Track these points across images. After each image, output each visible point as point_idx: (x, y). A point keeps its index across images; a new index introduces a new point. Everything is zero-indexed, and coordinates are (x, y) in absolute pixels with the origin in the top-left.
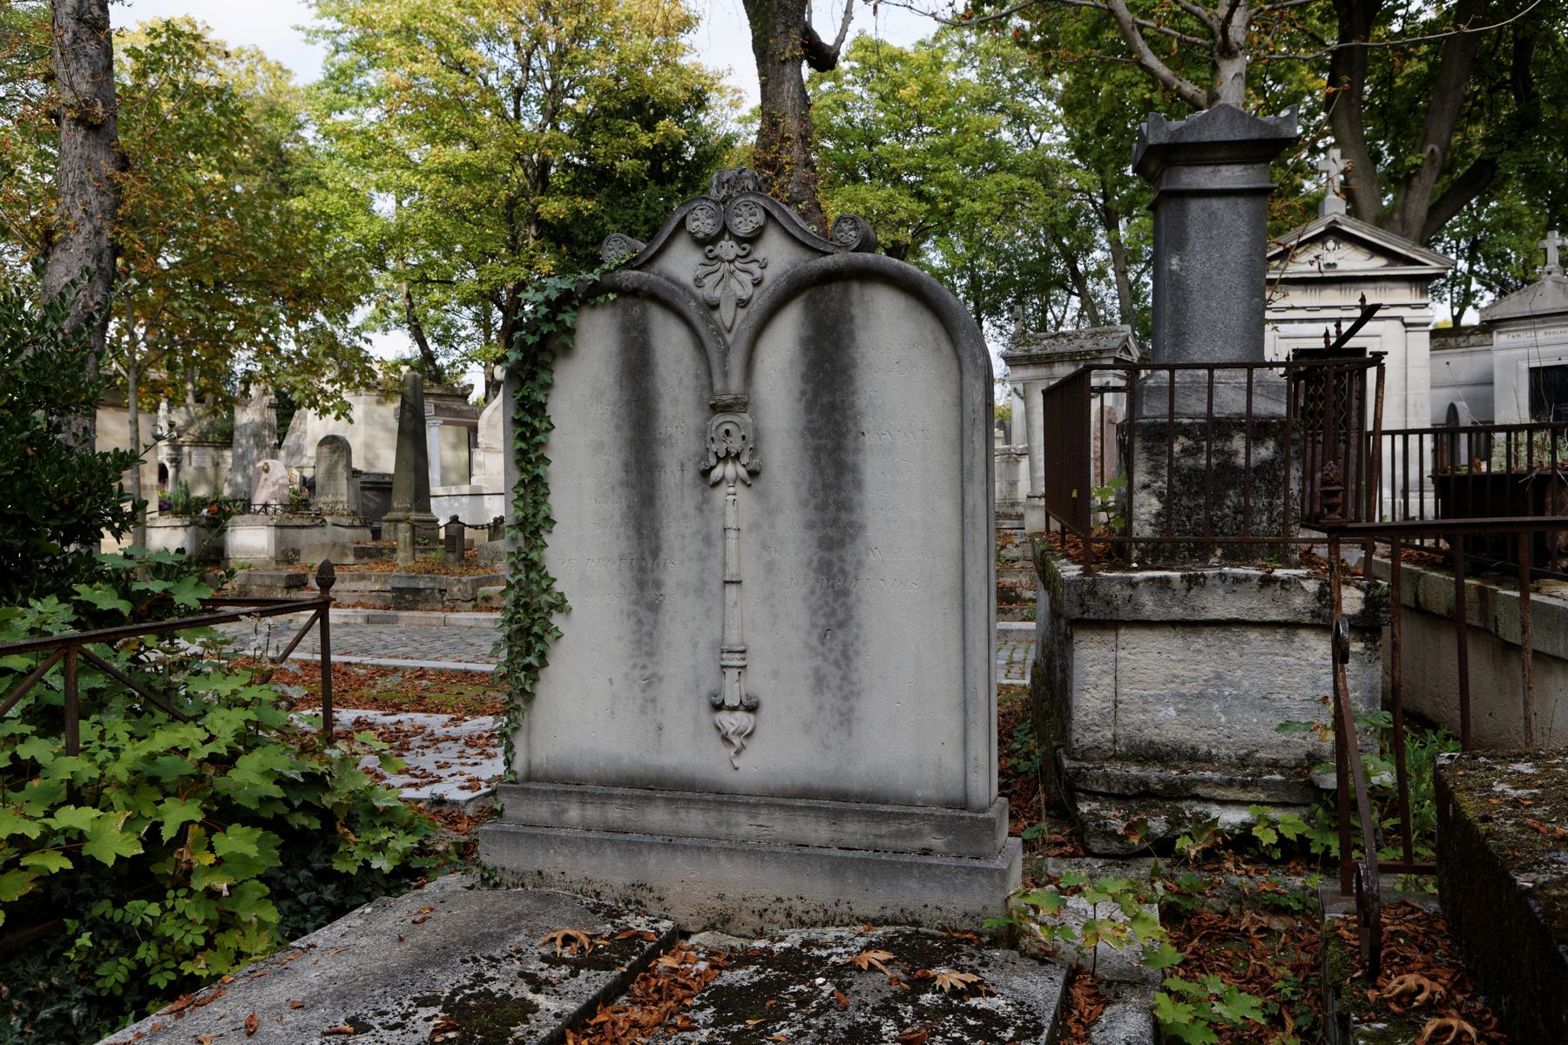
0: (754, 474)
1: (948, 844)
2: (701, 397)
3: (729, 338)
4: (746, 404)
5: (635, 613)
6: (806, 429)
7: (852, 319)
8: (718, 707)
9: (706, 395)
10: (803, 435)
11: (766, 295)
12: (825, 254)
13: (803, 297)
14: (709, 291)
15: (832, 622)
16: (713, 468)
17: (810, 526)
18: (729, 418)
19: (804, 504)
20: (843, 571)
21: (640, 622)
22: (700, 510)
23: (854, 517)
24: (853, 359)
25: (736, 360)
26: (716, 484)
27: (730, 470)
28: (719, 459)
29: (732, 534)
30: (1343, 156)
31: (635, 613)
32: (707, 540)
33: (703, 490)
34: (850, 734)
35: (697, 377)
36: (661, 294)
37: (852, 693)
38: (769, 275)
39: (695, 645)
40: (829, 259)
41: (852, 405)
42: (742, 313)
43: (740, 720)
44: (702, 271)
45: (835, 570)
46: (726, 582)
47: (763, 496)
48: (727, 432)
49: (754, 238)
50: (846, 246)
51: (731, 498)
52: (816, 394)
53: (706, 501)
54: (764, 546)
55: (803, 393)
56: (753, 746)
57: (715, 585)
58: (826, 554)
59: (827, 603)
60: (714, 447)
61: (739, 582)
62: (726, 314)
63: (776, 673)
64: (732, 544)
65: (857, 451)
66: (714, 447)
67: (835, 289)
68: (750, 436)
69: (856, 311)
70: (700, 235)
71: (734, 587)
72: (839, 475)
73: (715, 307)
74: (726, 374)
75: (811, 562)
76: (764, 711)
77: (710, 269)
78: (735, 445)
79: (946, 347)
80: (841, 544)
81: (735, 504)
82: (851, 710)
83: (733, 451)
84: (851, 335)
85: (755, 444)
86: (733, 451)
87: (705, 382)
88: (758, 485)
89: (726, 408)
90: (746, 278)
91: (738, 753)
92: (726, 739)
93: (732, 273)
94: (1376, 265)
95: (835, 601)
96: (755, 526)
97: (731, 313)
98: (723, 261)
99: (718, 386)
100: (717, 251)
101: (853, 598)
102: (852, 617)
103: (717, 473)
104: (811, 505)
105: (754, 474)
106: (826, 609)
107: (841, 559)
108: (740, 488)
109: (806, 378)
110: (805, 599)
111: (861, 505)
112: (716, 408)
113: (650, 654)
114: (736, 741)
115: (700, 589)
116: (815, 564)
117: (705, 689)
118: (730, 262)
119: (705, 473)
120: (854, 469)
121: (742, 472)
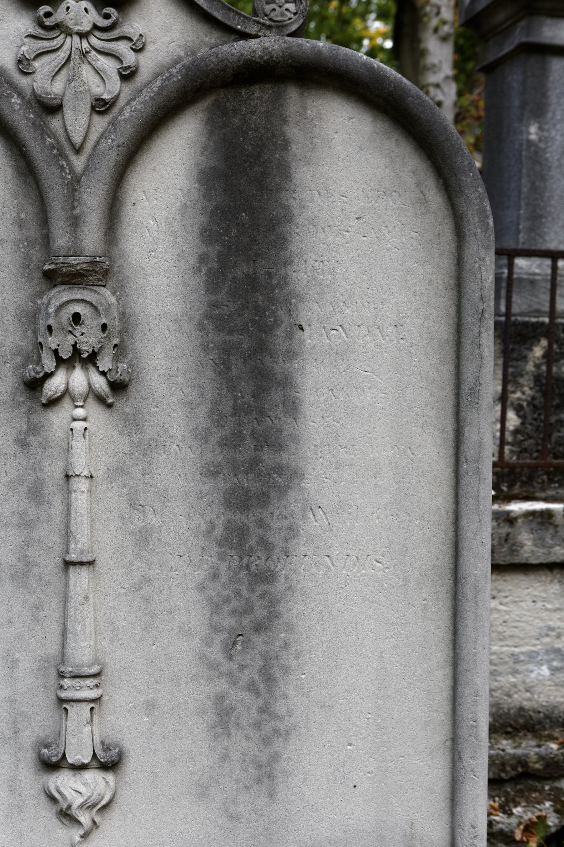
0: (118, 387)
2: (27, 258)
3: (78, 163)
4: (106, 273)
6: (206, 316)
7: (286, 144)
8: (50, 766)
9: (36, 254)
10: (201, 327)
11: (147, 95)
12: (246, 36)
13: (207, 103)
14: (45, 80)
15: (246, 622)
16: (49, 376)
18: (78, 294)
19: (203, 436)
20: (265, 543)
22: (23, 443)
23: (285, 458)
24: (287, 209)
25: (93, 200)
26: (53, 402)
27: (78, 379)
28: (60, 361)
29: (82, 485)
32: (36, 494)
33: (29, 412)
34: (272, 795)
35: (20, 223)
37: (276, 732)
38: (148, 63)
39: (13, 665)
40: (253, 43)
41: (284, 282)
42: (100, 123)
43: (95, 783)
44: (29, 48)
45: (253, 541)
46: (68, 564)
47: (133, 423)
48: (76, 318)
50: (278, 27)
51: (79, 425)
52: (224, 263)
53: (34, 429)
54: (134, 504)
55: (203, 259)
56: (111, 824)
57: (50, 567)
58: (238, 517)
59: (237, 593)
60: (52, 342)
61: (91, 563)
62: (76, 121)
63: (151, 706)
64: (81, 501)
65: (291, 354)
66: (52, 342)
67: (259, 95)
68: (115, 325)
69: (293, 132)
71: (84, 572)
72: (260, 392)
74: (75, 222)
75: (212, 527)
76: (132, 767)
77: (46, 45)
79: (436, 199)
80: (263, 500)
81: (85, 434)
82: (275, 758)
83: (86, 349)
84: (285, 171)
85: (121, 336)
86: (86, 349)
87: (34, 232)
88: (125, 406)
89: (75, 278)
90: (109, 66)
91: (84, 836)
92: (66, 815)
93: (84, 55)
95: (252, 589)
96: (118, 471)
97: (84, 122)
98: (69, 33)
99: (61, 240)
100: (60, 15)
101: (281, 585)
102: (278, 615)
103: (56, 384)
104: (214, 440)
105: (118, 387)
106: (236, 603)
107: (262, 524)
108: (93, 410)
109: (207, 235)
110: (201, 588)
111: (295, 439)
112: (53, 278)
114: (85, 818)
115: (23, 573)
116: (219, 531)
117: (28, 736)
118: (83, 35)
119: (34, 385)
120: (286, 383)
121: (100, 383)
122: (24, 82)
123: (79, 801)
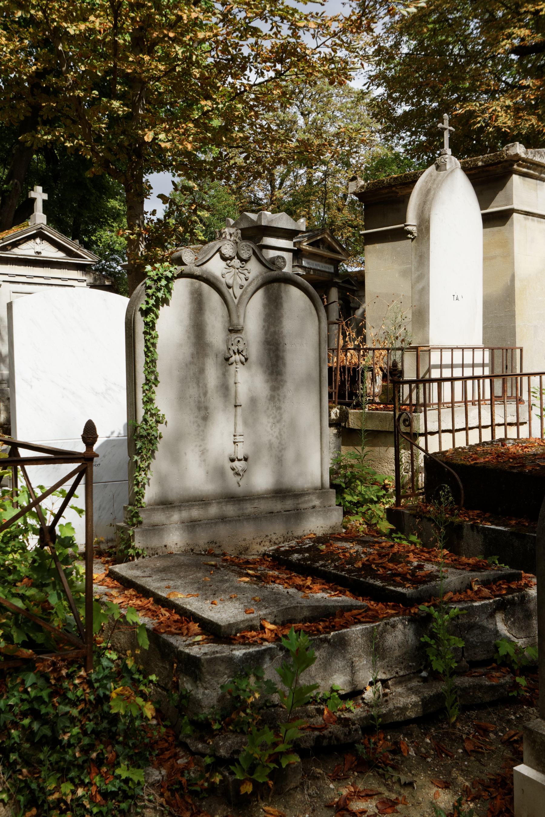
0: (246, 359)
1: (321, 503)
5: (196, 422)
9: (227, 325)
17: (267, 381)
18: (239, 335)
20: (279, 400)
21: (199, 426)
26: (232, 364)
27: (237, 357)
28: (235, 353)
30: (44, 191)
31: (196, 422)
35: (223, 317)
36: (212, 279)
38: (251, 276)
40: (276, 272)
42: (241, 291)
44: (225, 271)
49: (246, 261)
52: (269, 327)
55: (264, 326)
60: (233, 348)
65: (284, 351)
66: (233, 348)
67: (276, 285)
69: (283, 295)
70: (227, 256)
72: (277, 361)
73: (229, 287)
74: (238, 317)
76: (249, 460)
78: (241, 347)
79: (314, 312)
80: (278, 388)
90: (243, 276)
94: (59, 255)
99: (235, 320)
101: (283, 411)
105: (246, 359)
107: (278, 395)
108: (240, 365)
112: (230, 331)
113: (203, 440)
119: (227, 359)
120: (283, 358)
121: (243, 359)
122: (223, 280)
123: (240, 469)
